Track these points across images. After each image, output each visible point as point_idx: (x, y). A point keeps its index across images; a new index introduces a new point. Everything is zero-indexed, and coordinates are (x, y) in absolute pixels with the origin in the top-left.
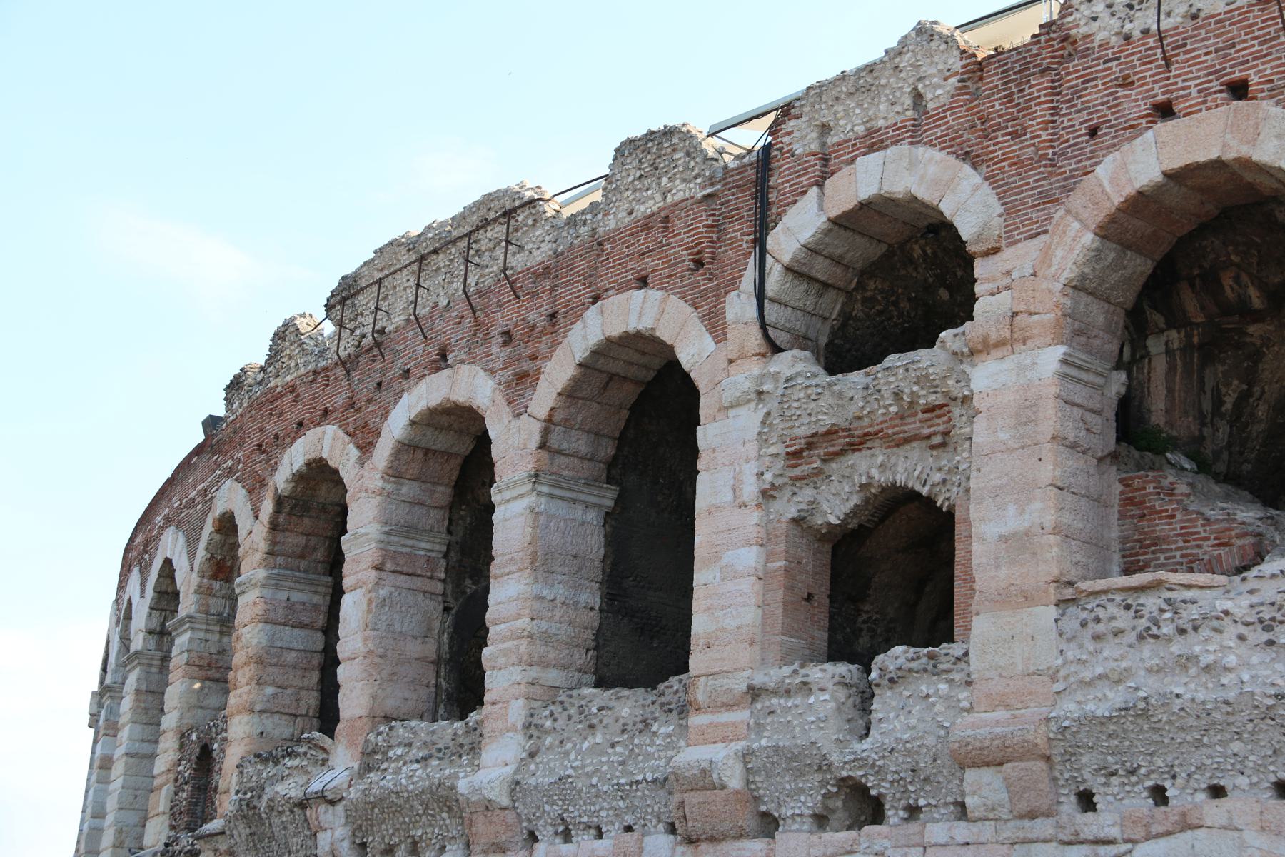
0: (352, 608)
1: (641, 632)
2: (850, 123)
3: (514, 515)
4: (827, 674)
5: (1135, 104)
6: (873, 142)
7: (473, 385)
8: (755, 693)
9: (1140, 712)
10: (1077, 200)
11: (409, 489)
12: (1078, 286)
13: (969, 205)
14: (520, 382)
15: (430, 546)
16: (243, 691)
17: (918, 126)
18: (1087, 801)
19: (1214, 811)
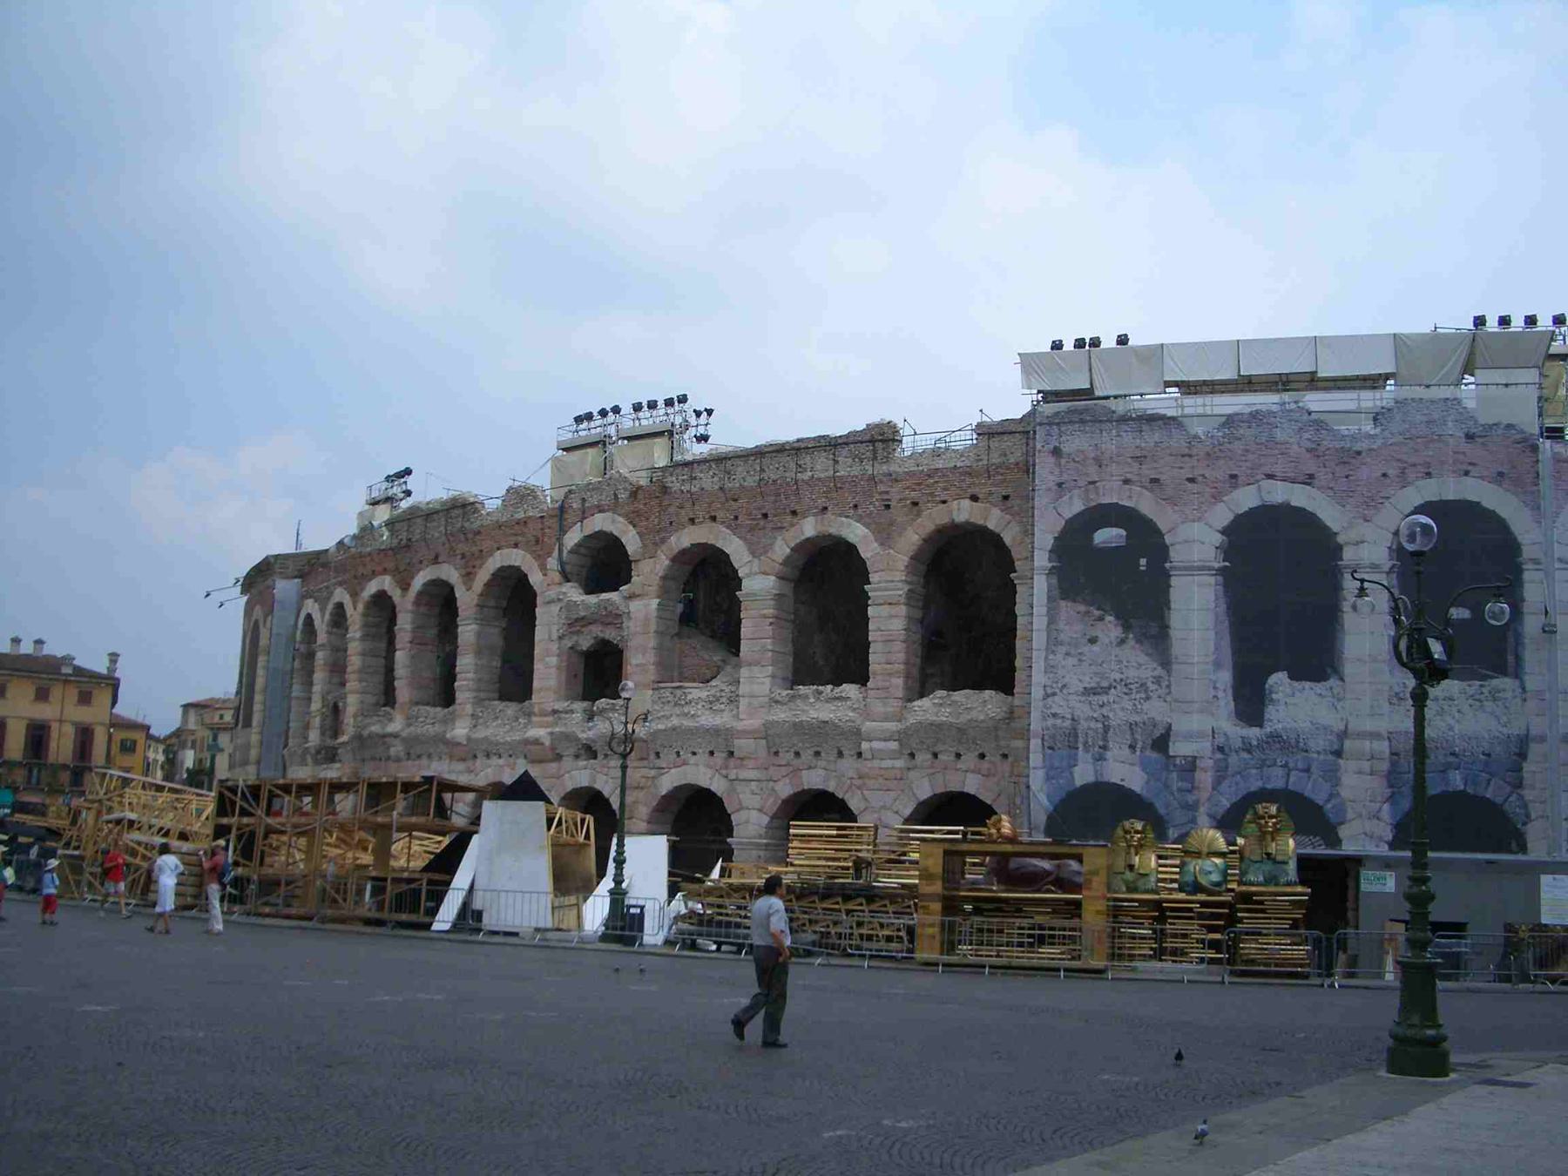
0: (400, 656)
1: (514, 682)
2: (593, 500)
3: (467, 632)
4: (579, 706)
5: (684, 515)
6: (601, 509)
7: (450, 573)
8: (555, 712)
9: (674, 729)
10: (664, 547)
11: (423, 609)
12: (664, 578)
13: (631, 541)
14: (468, 576)
15: (432, 633)
16: (352, 684)
17: (614, 506)
18: (658, 754)
19: (693, 760)
